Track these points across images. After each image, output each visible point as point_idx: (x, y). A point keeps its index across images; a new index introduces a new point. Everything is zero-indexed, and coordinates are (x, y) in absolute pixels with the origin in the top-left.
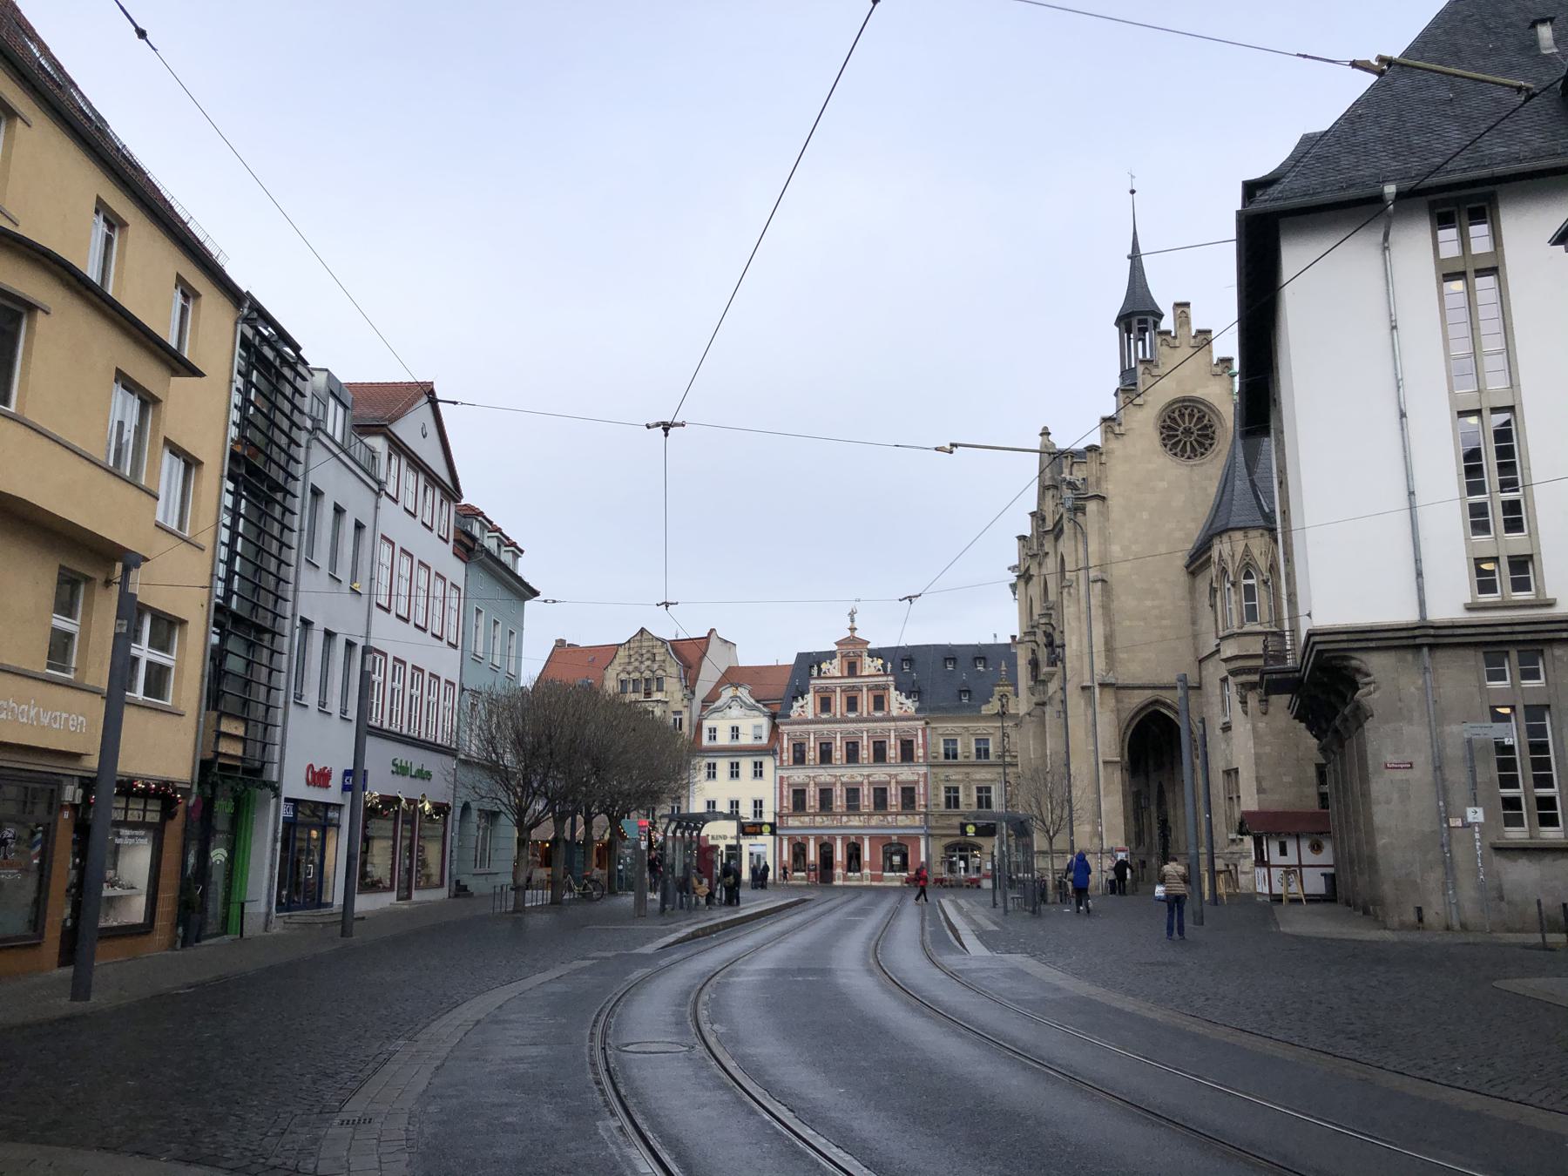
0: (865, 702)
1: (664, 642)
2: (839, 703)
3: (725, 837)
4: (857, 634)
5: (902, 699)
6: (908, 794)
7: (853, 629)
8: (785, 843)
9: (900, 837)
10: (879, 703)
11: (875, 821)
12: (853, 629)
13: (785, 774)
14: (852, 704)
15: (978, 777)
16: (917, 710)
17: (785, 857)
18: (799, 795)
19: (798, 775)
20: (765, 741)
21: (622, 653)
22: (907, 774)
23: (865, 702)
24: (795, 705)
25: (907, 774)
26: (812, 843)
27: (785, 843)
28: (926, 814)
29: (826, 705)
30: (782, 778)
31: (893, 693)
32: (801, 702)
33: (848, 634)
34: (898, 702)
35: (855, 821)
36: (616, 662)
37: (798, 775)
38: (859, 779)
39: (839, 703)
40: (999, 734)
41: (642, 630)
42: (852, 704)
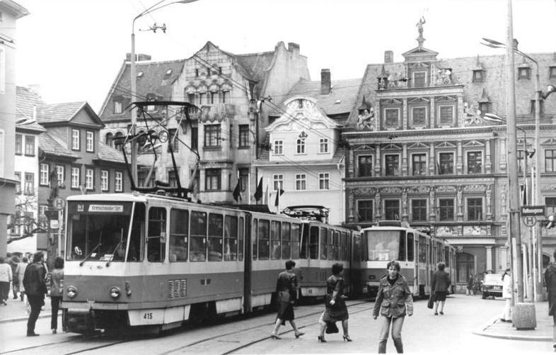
1: (230, 56)
4: (426, 46)
7: (421, 40)
9: (465, 246)
12: (421, 40)
21: (191, 67)
33: (415, 45)
36: (184, 75)
37: (364, 187)
41: (208, 46)
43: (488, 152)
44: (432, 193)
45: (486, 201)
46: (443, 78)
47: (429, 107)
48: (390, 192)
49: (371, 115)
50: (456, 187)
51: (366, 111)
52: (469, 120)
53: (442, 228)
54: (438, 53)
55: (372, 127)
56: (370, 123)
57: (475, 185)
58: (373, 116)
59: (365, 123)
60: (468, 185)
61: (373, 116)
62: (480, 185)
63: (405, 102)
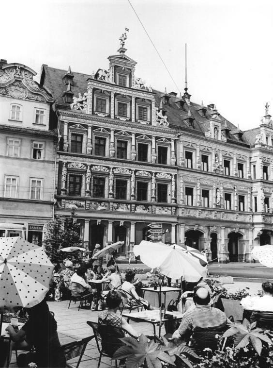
0: (132, 110)
2: (111, 107)
5: (160, 114)
6: (162, 190)
7: (122, 51)
11: (140, 210)
12: (122, 51)
13: (65, 159)
14: (122, 108)
15: (204, 182)
16: (170, 126)
18: (75, 178)
19: (77, 163)
23: (132, 110)
33: (118, 53)
35: (123, 209)
38: (129, 173)
39: (111, 107)
42: (122, 108)
43: (173, 149)
44: (133, 175)
45: (170, 189)
46: (141, 85)
47: (131, 105)
48: (99, 170)
49: (84, 99)
50: (151, 173)
51: (80, 94)
52: (159, 122)
53: (139, 207)
56: (83, 105)
57: (163, 174)
58: (86, 101)
59: (79, 104)
60: (160, 173)
61: (86, 101)
63: (112, 96)
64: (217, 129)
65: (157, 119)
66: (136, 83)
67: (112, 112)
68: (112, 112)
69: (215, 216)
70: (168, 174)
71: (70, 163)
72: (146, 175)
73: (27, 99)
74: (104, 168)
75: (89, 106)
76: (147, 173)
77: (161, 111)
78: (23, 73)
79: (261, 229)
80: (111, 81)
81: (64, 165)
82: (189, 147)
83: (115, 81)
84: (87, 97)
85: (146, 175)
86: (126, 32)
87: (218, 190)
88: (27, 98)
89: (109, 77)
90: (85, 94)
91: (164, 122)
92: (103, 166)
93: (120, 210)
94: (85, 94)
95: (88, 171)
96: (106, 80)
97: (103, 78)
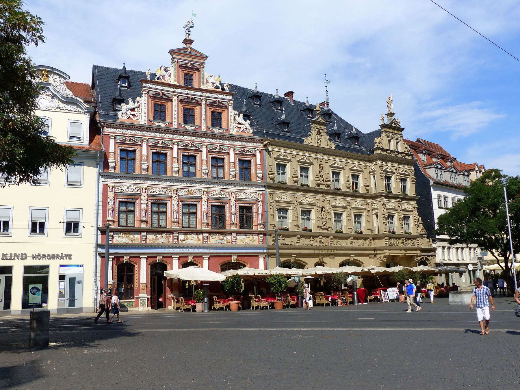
0: (203, 116)
2: (174, 113)
3: (24, 257)
5: (241, 119)
7: (188, 42)
8: (110, 263)
10: (217, 120)
11: (214, 240)
14: (189, 116)
17: (110, 280)
19: (128, 186)
20: (85, 141)
22: (247, 193)
23: (203, 116)
24: (124, 107)
25: (247, 193)
26: (143, 263)
27: (110, 263)
28: (265, 234)
29: (159, 112)
30: (106, 187)
31: (232, 113)
32: (131, 105)
34: (234, 122)
35: (193, 239)
37: (128, 186)
38: (198, 194)
39: (174, 113)
40: (316, 164)
42: (189, 116)
43: (259, 162)
44: (205, 197)
48: (158, 193)
49: (136, 105)
51: (130, 100)
54: (206, 58)
55: (136, 118)
56: (135, 113)
58: (139, 107)
61: (139, 107)
62: (252, 193)
64: (320, 133)
65: (237, 125)
66: (207, 82)
67: (175, 120)
68: (175, 120)
69: (321, 242)
70: (252, 193)
71: (119, 186)
72: (223, 196)
73: (58, 110)
74: (164, 190)
75: (143, 113)
76: (223, 193)
77: (242, 115)
78: (51, 77)
79: (383, 255)
80: (173, 82)
81: (111, 190)
82: (281, 157)
83: (178, 81)
84: (140, 102)
85: (223, 195)
86: (193, 18)
87: (324, 209)
88: (57, 108)
89: (170, 76)
90: (138, 99)
91: (246, 128)
92: (164, 188)
93: (189, 242)
94: (138, 99)
95: (143, 194)
96: (167, 80)
97: (161, 77)
